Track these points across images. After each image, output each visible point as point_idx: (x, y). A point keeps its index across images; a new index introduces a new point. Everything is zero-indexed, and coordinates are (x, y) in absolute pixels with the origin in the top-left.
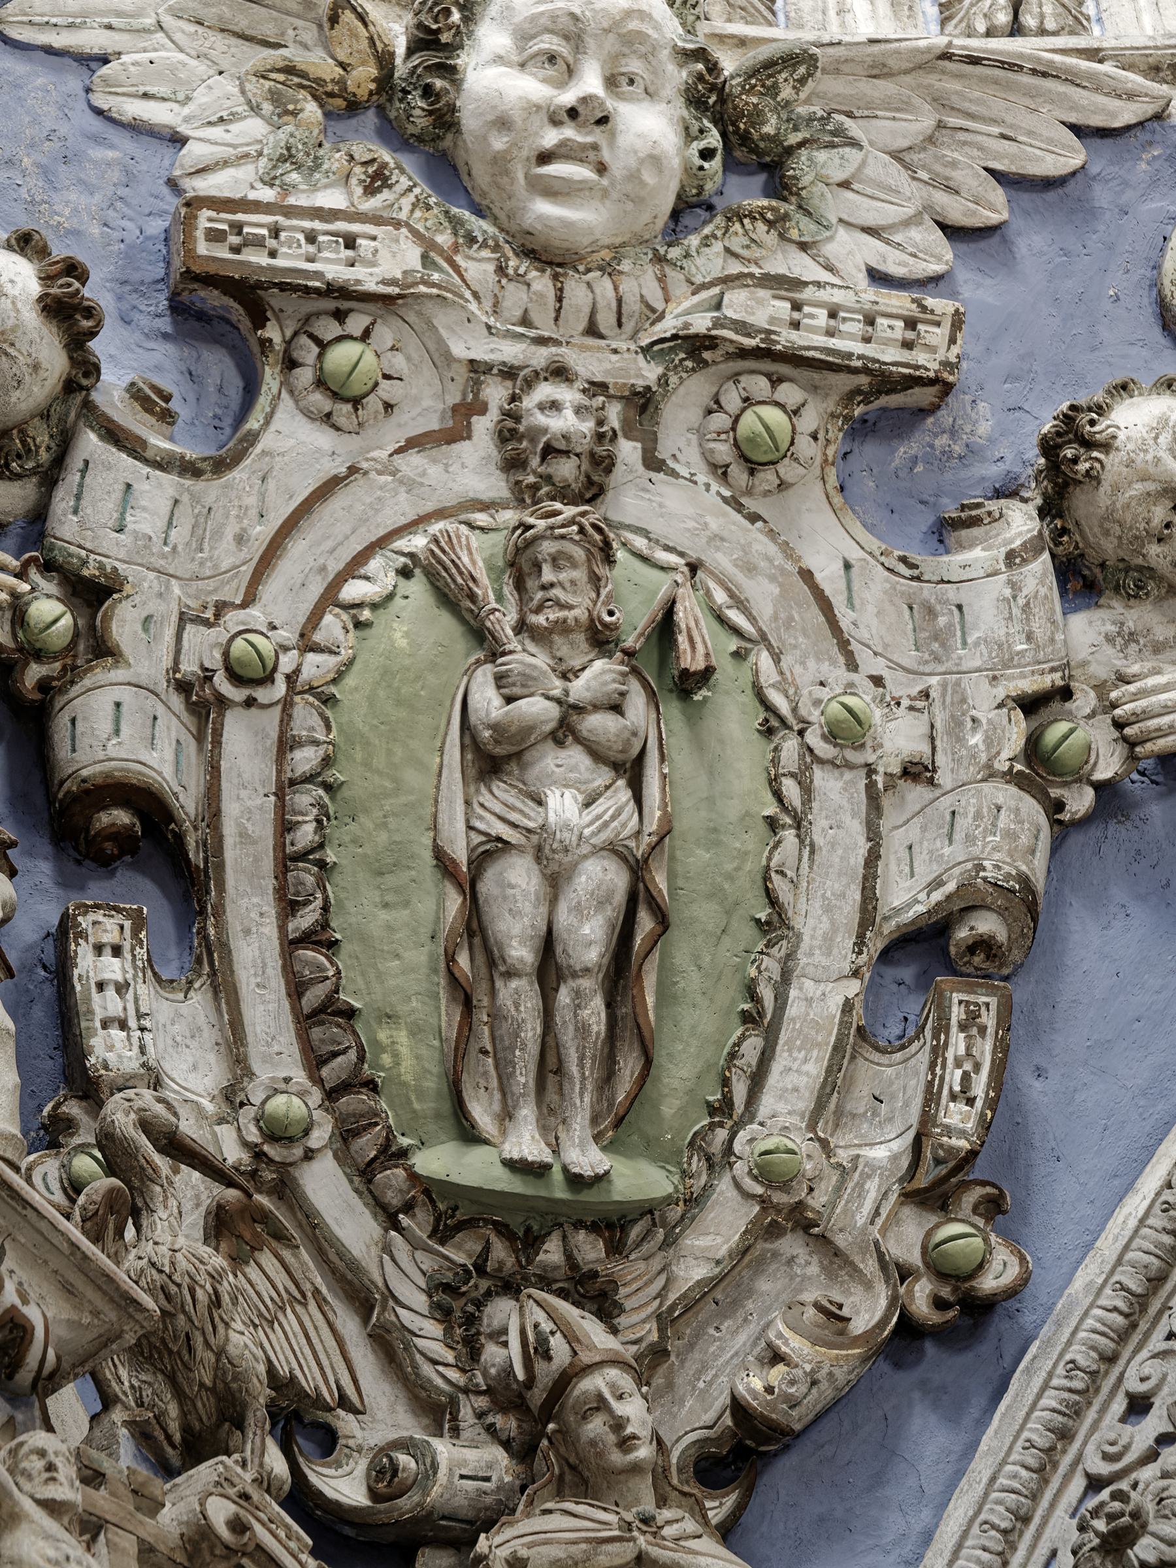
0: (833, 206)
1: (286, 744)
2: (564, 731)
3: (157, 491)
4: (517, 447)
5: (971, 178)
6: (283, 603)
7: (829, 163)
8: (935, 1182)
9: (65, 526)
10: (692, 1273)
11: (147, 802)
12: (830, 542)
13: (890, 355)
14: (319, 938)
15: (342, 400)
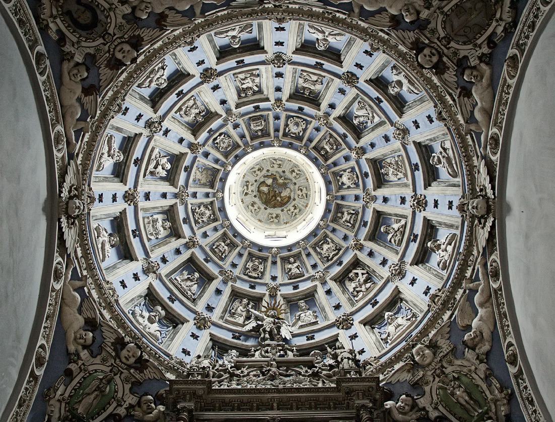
0: (441, 345)
1: (442, 406)
2: (454, 389)
3: (422, 400)
4: (439, 376)
5: (446, 335)
6: (435, 397)
7: (438, 343)
8: (501, 391)
9: (420, 407)
10: (494, 411)
11: (437, 417)
12: (458, 362)
13: (450, 349)
14: (455, 414)
15: (427, 383)
